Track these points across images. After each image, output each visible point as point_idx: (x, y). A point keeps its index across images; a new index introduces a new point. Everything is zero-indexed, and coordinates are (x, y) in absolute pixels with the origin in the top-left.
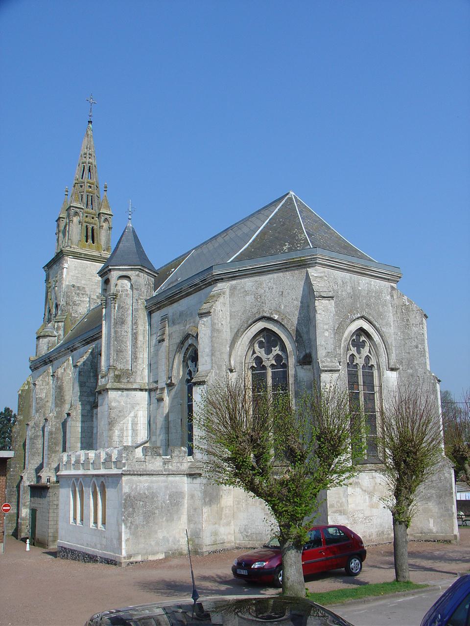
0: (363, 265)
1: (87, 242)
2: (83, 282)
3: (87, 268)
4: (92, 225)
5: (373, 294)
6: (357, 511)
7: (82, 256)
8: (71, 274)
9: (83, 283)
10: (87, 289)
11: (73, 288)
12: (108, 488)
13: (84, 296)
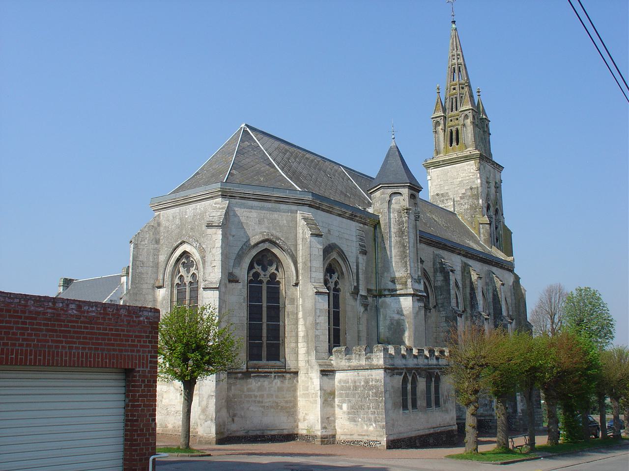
0: (183, 197)
1: (451, 146)
2: (446, 188)
3: (448, 173)
4: (456, 127)
5: (198, 217)
6: (170, 405)
7: (441, 163)
8: (435, 184)
9: (446, 189)
10: (450, 194)
11: (437, 197)
12: (399, 388)
13: (449, 201)
